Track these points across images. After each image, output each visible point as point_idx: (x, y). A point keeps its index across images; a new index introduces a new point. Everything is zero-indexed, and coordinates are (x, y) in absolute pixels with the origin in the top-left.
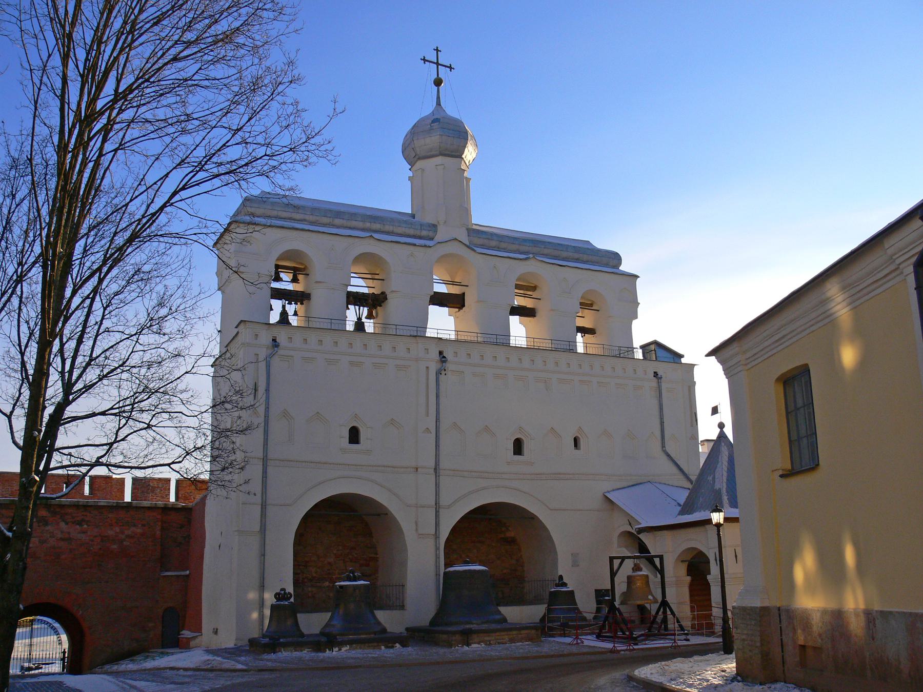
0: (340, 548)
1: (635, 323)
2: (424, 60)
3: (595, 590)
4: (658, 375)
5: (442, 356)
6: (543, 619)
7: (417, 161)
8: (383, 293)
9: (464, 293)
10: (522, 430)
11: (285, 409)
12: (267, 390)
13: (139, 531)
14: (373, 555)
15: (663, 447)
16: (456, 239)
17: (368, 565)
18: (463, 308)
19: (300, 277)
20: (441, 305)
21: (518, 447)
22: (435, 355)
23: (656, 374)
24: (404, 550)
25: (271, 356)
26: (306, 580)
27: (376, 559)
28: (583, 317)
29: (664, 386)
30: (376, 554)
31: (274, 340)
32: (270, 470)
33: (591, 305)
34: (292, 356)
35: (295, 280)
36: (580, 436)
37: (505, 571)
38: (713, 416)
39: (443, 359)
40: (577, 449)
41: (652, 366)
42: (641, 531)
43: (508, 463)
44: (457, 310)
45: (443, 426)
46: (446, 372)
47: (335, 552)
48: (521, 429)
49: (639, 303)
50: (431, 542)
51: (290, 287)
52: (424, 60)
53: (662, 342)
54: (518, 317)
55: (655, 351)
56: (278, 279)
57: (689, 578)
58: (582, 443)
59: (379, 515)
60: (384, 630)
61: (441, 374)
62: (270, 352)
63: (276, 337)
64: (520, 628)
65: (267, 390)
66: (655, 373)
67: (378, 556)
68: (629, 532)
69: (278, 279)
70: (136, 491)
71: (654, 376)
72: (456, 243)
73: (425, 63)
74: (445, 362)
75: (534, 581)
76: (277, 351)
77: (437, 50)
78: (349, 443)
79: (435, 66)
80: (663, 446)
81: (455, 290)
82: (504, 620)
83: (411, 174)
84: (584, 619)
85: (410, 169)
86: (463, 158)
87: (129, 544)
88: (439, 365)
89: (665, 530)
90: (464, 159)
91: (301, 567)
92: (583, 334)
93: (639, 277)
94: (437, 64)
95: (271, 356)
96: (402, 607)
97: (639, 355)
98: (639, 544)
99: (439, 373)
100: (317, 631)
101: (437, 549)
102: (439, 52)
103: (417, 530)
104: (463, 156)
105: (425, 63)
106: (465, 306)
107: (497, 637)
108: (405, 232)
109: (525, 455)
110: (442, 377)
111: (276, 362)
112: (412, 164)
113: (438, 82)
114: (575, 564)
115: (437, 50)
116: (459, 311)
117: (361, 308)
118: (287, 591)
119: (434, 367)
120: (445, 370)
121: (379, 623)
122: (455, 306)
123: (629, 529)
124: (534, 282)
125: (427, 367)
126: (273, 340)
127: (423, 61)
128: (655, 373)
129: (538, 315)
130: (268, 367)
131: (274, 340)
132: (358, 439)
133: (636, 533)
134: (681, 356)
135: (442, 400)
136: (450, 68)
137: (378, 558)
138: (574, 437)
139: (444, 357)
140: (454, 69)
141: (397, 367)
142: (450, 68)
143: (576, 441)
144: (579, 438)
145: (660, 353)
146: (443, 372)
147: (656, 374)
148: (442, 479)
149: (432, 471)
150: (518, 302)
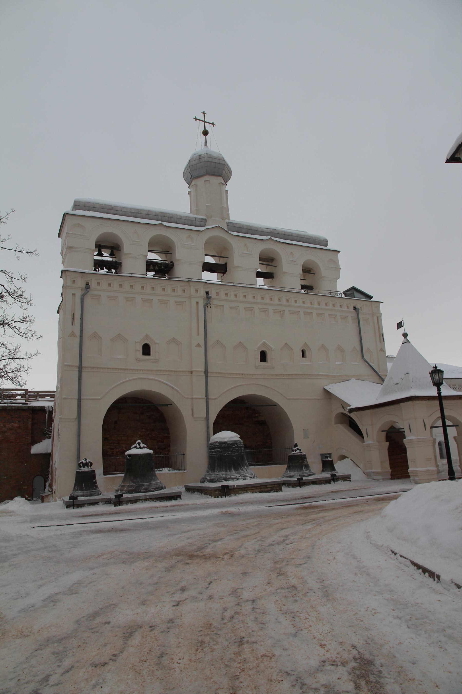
0: (144, 430)
2: (196, 119)
3: (321, 454)
4: (356, 308)
9: (226, 264)
10: (265, 345)
11: (95, 332)
12: (82, 318)
13: (16, 425)
14: (166, 435)
16: (218, 227)
18: (226, 273)
21: (263, 357)
22: (203, 293)
23: (355, 308)
26: (119, 453)
27: (168, 438)
28: (305, 280)
30: (169, 434)
31: (87, 284)
32: (84, 375)
34: (101, 295)
35: (112, 255)
42: (351, 411)
43: (257, 367)
44: (222, 274)
45: (210, 344)
46: (211, 305)
47: (139, 433)
52: (196, 119)
54: (263, 279)
55: (354, 294)
56: (100, 254)
57: (387, 443)
58: (307, 354)
59: (167, 405)
61: (207, 307)
62: (83, 292)
63: (88, 282)
65: (82, 318)
66: (354, 307)
67: (170, 435)
69: (100, 254)
71: (354, 310)
77: (204, 113)
80: (363, 356)
81: (222, 262)
85: (189, 187)
87: (9, 434)
91: (115, 444)
92: (305, 290)
93: (339, 252)
94: (205, 122)
99: (205, 306)
101: (208, 428)
102: (205, 115)
103: (193, 415)
109: (268, 361)
110: (208, 309)
111: (88, 301)
112: (189, 183)
113: (205, 133)
115: (204, 113)
116: (224, 275)
120: (210, 304)
125: (197, 303)
126: (86, 284)
128: (354, 307)
131: (87, 284)
134: (371, 297)
136: (213, 124)
137: (170, 436)
141: (176, 303)
142: (213, 124)
143: (303, 353)
144: (305, 351)
146: (209, 306)
147: (355, 308)
148: (210, 379)
149: (203, 374)
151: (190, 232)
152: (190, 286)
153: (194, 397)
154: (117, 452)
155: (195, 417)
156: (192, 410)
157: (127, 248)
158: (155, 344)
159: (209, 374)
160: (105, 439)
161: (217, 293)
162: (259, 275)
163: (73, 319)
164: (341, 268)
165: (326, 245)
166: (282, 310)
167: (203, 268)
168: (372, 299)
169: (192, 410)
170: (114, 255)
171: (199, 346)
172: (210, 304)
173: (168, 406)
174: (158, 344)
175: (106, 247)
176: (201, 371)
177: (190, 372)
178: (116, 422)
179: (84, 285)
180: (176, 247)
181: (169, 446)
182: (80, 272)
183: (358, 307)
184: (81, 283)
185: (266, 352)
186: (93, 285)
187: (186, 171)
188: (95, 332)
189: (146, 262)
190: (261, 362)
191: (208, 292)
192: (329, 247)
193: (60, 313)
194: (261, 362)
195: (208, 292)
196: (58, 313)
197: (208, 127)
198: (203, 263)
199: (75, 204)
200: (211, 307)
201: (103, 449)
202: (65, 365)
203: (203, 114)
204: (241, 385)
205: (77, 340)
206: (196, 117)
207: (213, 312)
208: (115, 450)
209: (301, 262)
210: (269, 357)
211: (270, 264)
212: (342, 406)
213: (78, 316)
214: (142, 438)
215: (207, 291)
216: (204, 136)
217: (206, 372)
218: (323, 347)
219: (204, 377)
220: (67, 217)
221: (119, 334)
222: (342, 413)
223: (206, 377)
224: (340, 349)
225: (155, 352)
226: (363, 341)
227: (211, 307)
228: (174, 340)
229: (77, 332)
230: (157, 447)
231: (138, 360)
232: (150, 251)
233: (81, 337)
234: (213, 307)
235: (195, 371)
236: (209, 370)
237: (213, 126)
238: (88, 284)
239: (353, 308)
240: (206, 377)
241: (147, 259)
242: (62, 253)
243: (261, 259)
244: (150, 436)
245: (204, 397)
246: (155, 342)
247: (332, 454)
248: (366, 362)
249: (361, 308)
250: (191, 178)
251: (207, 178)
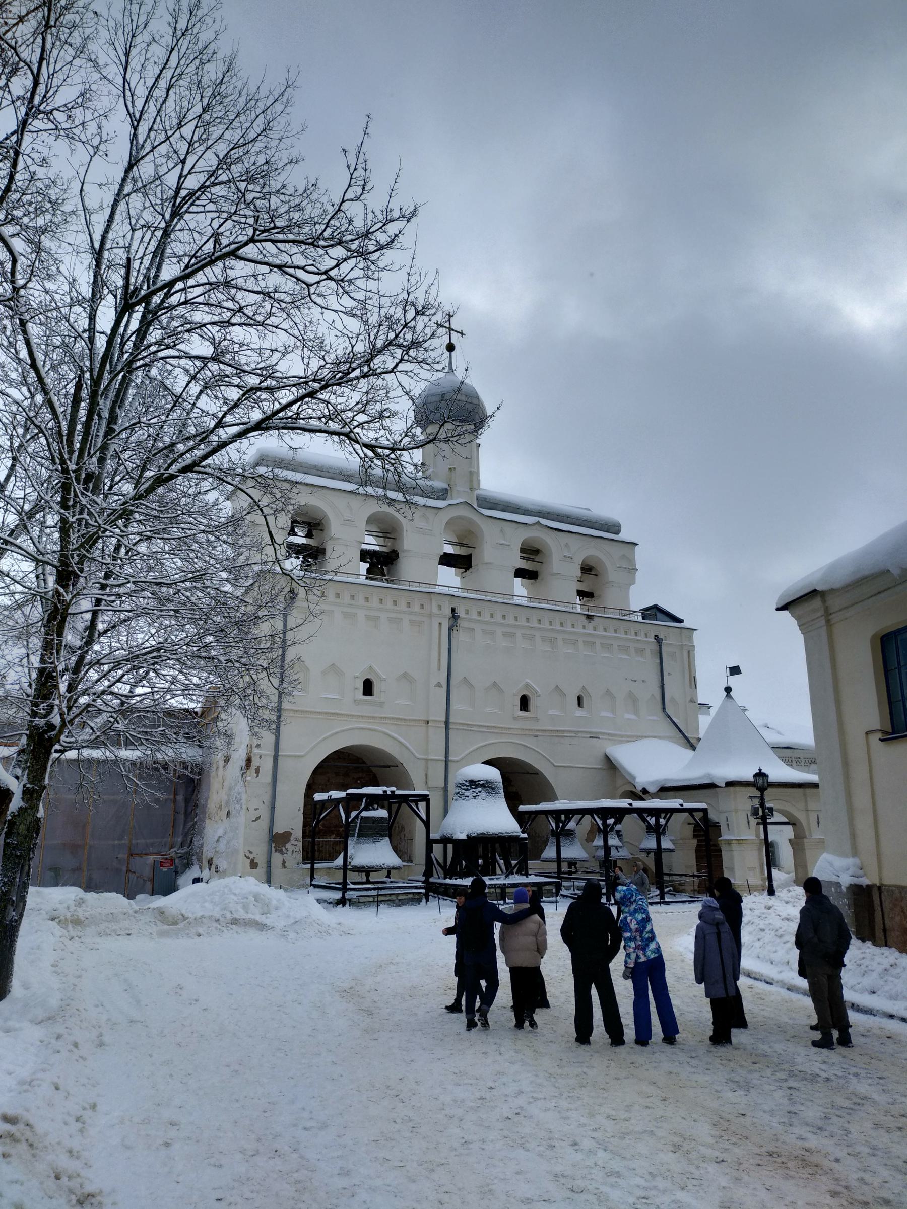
19: (315, 532)
20: (449, 565)
21: (524, 703)
35: (309, 535)
43: (515, 719)
44: (464, 570)
46: (458, 628)
48: (527, 685)
56: (292, 533)
58: (585, 702)
66: (655, 636)
80: (664, 708)
93: (637, 544)
99: (450, 629)
103: (426, 782)
110: (454, 633)
116: (465, 572)
124: (537, 546)
128: (655, 636)
136: (462, 334)
142: (462, 334)
146: (455, 628)
153: (430, 757)
156: (426, 775)
157: (335, 528)
159: (451, 726)
161: (467, 612)
165: (617, 532)
169: (426, 775)
171: (439, 685)
174: (385, 680)
176: (440, 721)
183: (661, 637)
190: (521, 710)
192: (622, 536)
194: (521, 710)
197: (455, 338)
204: (493, 743)
207: (460, 637)
209: (579, 561)
210: (532, 704)
217: (447, 723)
218: (608, 692)
222: (631, 792)
223: (447, 728)
226: (665, 686)
228: (405, 675)
240: (447, 728)
243: (523, 550)
248: (669, 717)
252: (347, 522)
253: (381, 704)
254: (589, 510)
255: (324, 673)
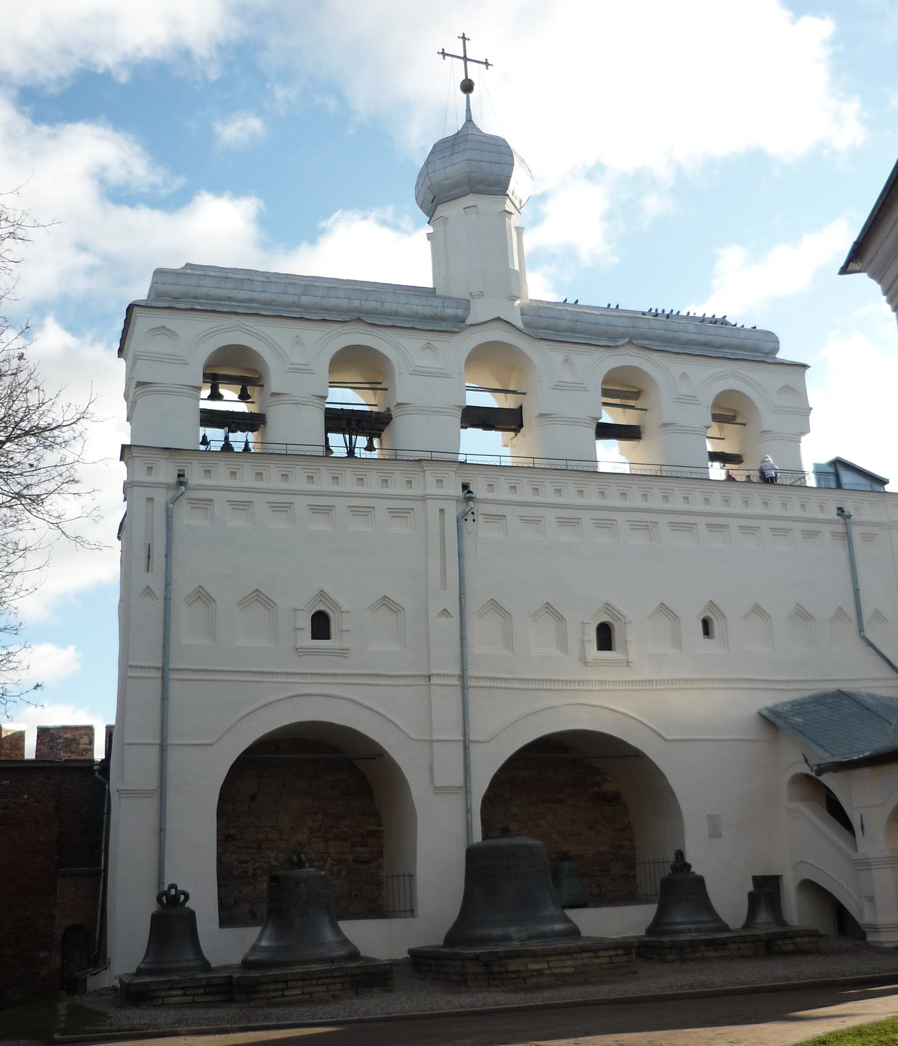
0: (320, 817)
1: (804, 439)
4: (843, 511)
5: (466, 491)
6: (650, 931)
7: (436, 207)
8: (389, 410)
9: (521, 407)
11: (200, 587)
12: (168, 556)
15: (860, 631)
16: (498, 319)
17: (364, 845)
18: (522, 430)
23: (841, 510)
24: (411, 813)
25: (175, 500)
26: (259, 872)
28: (723, 439)
29: (856, 532)
30: (381, 826)
32: (175, 688)
33: (734, 417)
34: (211, 500)
35: (244, 397)
36: (712, 617)
37: (601, 849)
38: (810, 366)
39: (469, 495)
40: (709, 638)
41: (833, 500)
42: (821, 770)
44: (512, 434)
47: (309, 824)
48: (608, 607)
49: (812, 409)
50: (456, 804)
51: (242, 407)
52: (444, 54)
53: (849, 461)
56: (215, 396)
58: (717, 627)
60: (355, 955)
61: (466, 520)
62: (171, 494)
63: (184, 470)
64: (599, 947)
67: (382, 829)
68: (807, 776)
69: (215, 396)
70: (42, 746)
71: (838, 515)
72: (501, 325)
73: (444, 58)
74: (471, 499)
75: (659, 862)
76: (183, 493)
77: (464, 38)
78: (312, 639)
79: (462, 62)
80: (861, 630)
82: (574, 932)
83: (431, 230)
84: (726, 928)
85: (429, 223)
86: (508, 195)
88: (462, 507)
89: (866, 766)
90: (510, 195)
91: (250, 851)
93: (810, 367)
95: (175, 500)
96: (411, 912)
97: (811, 481)
98: (827, 796)
99: (462, 518)
100: (236, 958)
101: (468, 811)
102: (467, 41)
104: (508, 192)
105: (444, 58)
106: (523, 426)
107: (551, 964)
108: (417, 313)
109: (617, 648)
113: (467, 87)
114: (715, 832)
115: (464, 38)
116: (516, 435)
117: (354, 437)
118: (179, 888)
119: (452, 510)
120: (473, 513)
121: (345, 942)
122: (509, 427)
123: (806, 770)
125: (442, 511)
126: (179, 476)
127: (441, 56)
129: (645, 436)
130: (169, 518)
132: (329, 631)
133: (813, 774)
134: (883, 482)
135: (468, 563)
137: (383, 831)
138: (702, 618)
139: (470, 492)
140: (491, 65)
142: (486, 63)
145: (847, 478)
146: (470, 517)
147: (841, 510)
148: (472, 694)
149: (456, 682)
150: (607, 417)
151: (429, 336)
152: (424, 471)
153: (435, 737)
154: (255, 869)
155: (436, 785)
156: (431, 768)
157: (276, 380)
158: (342, 612)
159: (471, 683)
160: (225, 839)
162: (605, 431)
163: (149, 557)
164: (812, 409)
166: (650, 522)
167: (462, 422)
168: (887, 488)
170: (249, 397)
172: (473, 513)
173: (374, 758)
175: (230, 380)
177: (427, 676)
178: (253, 798)
179: (172, 478)
180: (397, 372)
181: (381, 854)
182: (164, 448)
183: (849, 508)
184: (166, 473)
185: (613, 625)
186: (195, 477)
187: (420, 185)
188: (200, 587)
189: (326, 413)
191: (469, 483)
193: (123, 538)
195: (469, 483)
196: (119, 538)
197: (475, 73)
198: (463, 410)
199: (155, 281)
200: (476, 522)
201: (220, 862)
202: (131, 667)
203: (461, 40)
205: (159, 604)
206: (443, 49)
208: (250, 864)
209: (708, 398)
211: (631, 403)
212: (803, 759)
213: (159, 551)
214: (314, 835)
215: (464, 481)
216: (465, 96)
219: (459, 689)
220: (136, 310)
221: (257, 590)
223: (464, 688)
224: (802, 614)
225: (342, 631)
227: (474, 520)
228: (386, 602)
229: (158, 588)
230: (350, 857)
231: (300, 651)
232: (333, 384)
233: (167, 599)
234: (480, 519)
235: (438, 675)
236: (471, 672)
237: (487, 68)
238: (183, 476)
239: (835, 511)
240: (464, 688)
241: (327, 403)
242: (126, 396)
244: (335, 830)
245: (461, 738)
246: (340, 608)
247: (781, 876)
248: (871, 645)
249: (857, 509)
250: (433, 201)
251: (470, 200)
252: (305, 370)
253: (343, 653)
254: (723, 322)
255: (242, 604)
